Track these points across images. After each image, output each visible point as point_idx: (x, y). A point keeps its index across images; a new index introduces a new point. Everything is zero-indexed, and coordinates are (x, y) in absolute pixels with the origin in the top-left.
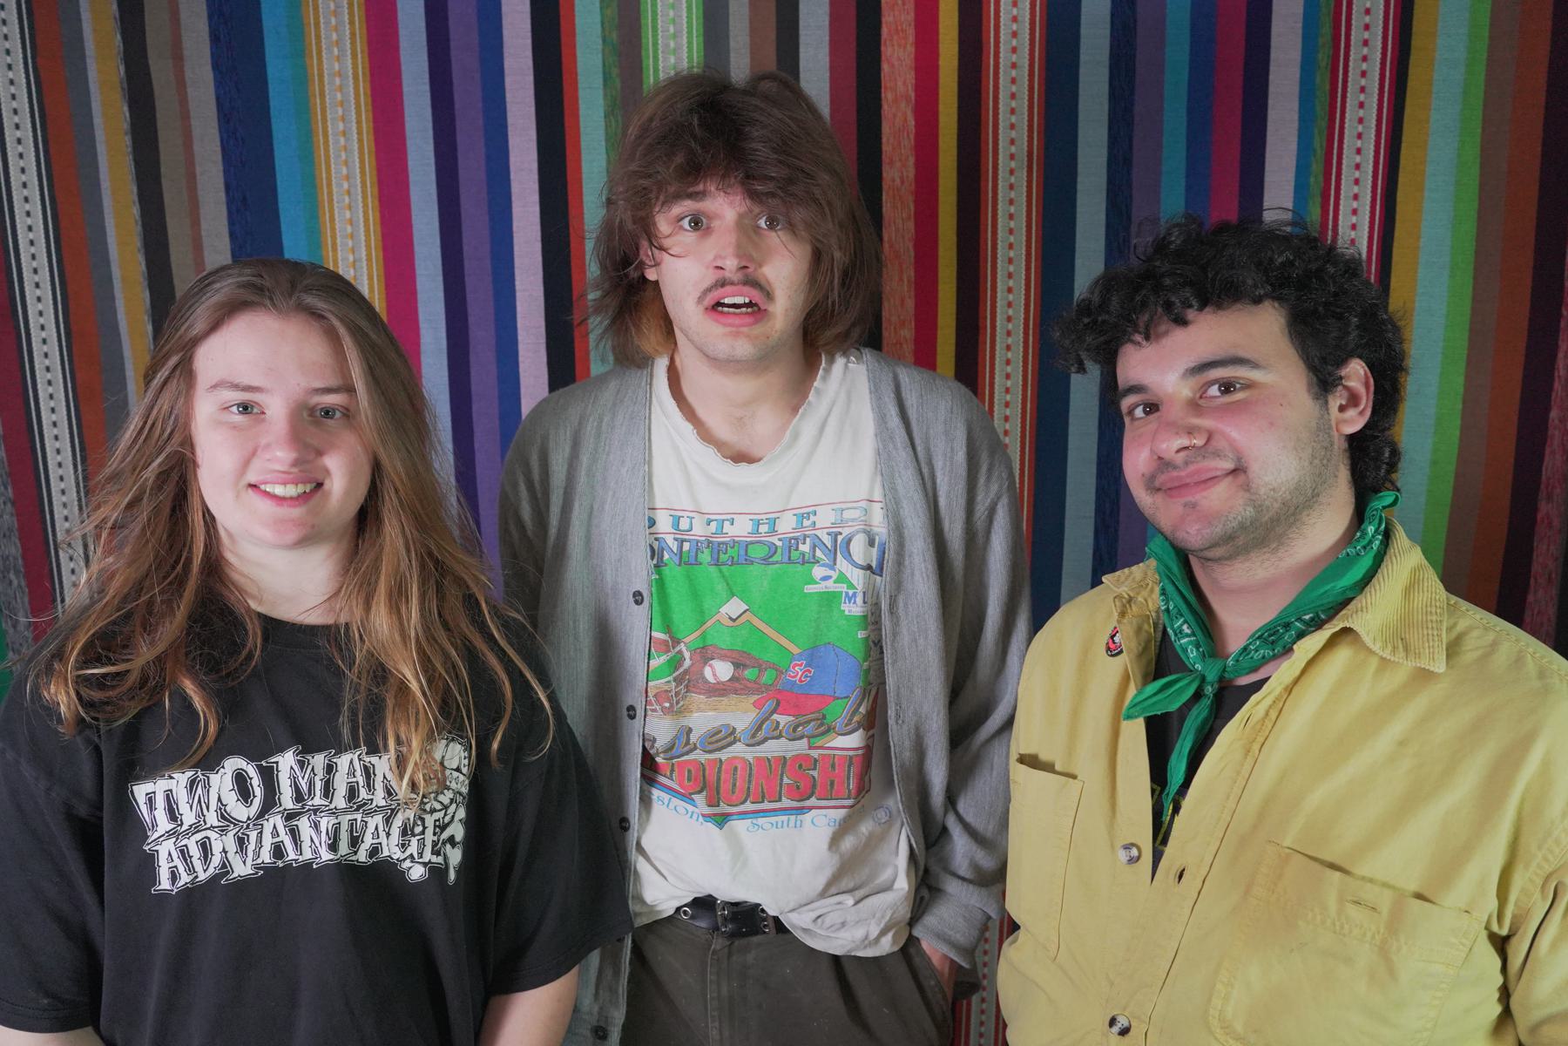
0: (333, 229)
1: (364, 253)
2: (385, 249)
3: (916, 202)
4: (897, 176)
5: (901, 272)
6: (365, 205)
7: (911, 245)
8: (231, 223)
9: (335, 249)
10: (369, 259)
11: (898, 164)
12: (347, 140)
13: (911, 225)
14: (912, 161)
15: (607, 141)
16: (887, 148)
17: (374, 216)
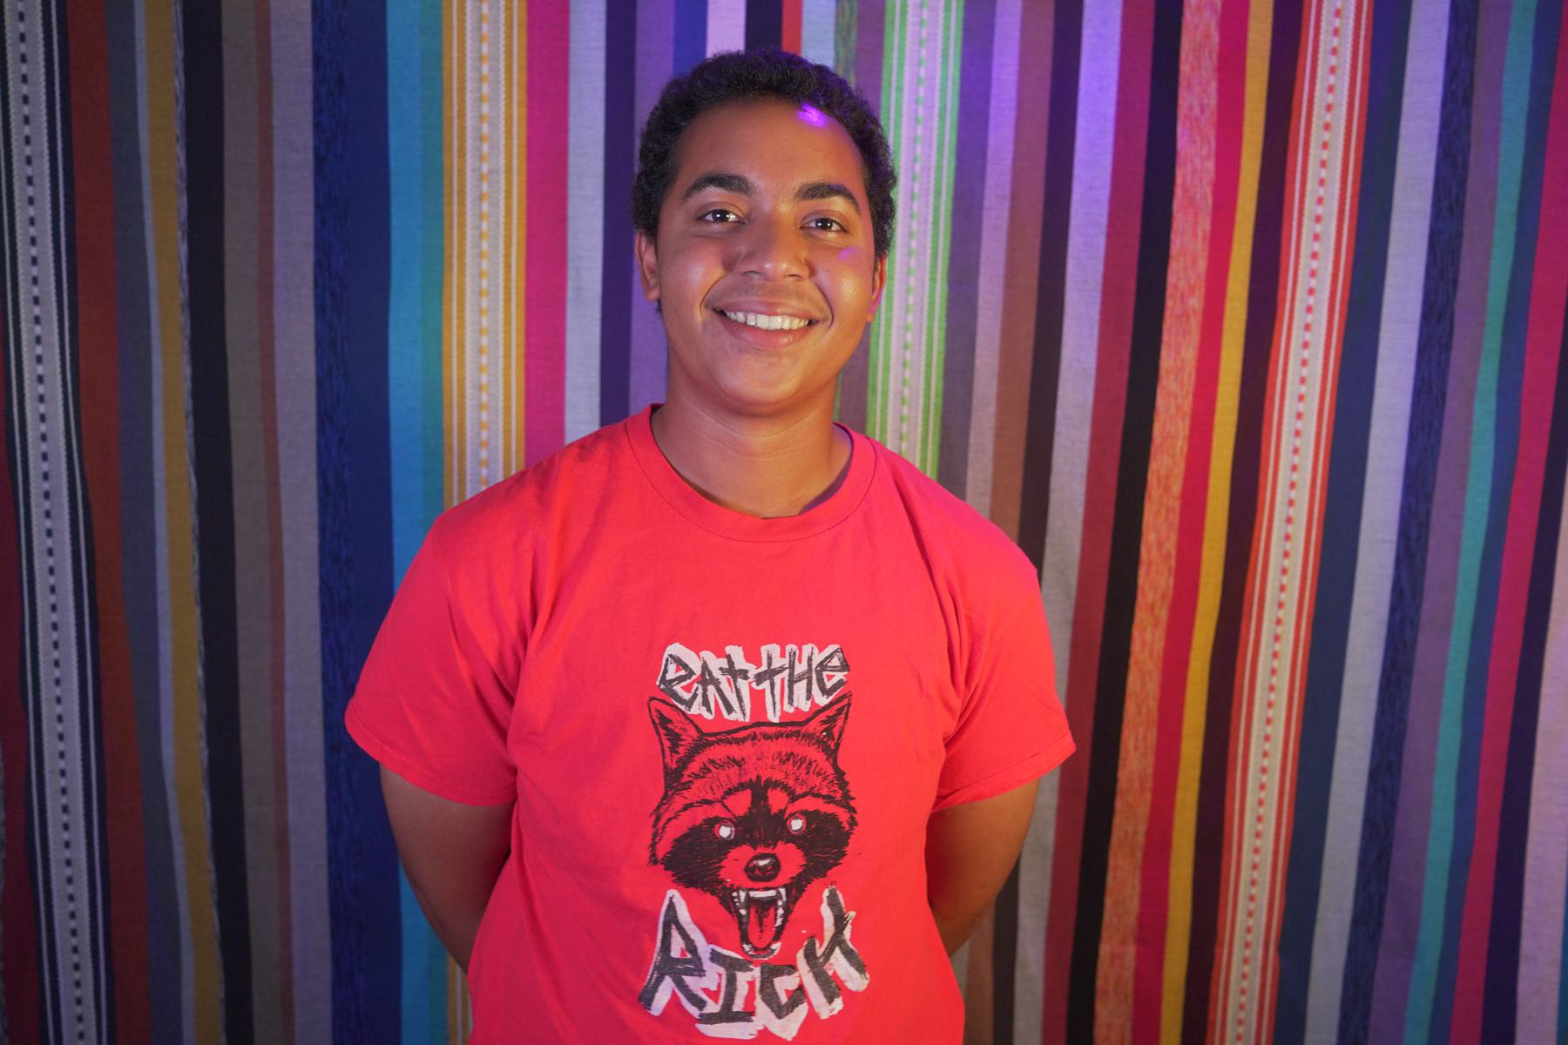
0: (462, 128)
1: (502, 162)
2: (531, 157)
3: (1219, 138)
4: (1196, 103)
5: (1196, 224)
6: (509, 98)
7: (1208, 190)
8: (318, 111)
9: (462, 155)
10: (509, 171)
11: (1197, 89)
12: (490, 7)
13: (1211, 165)
14: (1214, 85)
15: (837, 32)
16: (1185, 68)
17: (519, 112)
